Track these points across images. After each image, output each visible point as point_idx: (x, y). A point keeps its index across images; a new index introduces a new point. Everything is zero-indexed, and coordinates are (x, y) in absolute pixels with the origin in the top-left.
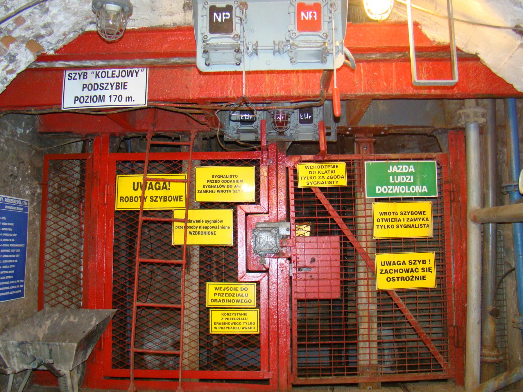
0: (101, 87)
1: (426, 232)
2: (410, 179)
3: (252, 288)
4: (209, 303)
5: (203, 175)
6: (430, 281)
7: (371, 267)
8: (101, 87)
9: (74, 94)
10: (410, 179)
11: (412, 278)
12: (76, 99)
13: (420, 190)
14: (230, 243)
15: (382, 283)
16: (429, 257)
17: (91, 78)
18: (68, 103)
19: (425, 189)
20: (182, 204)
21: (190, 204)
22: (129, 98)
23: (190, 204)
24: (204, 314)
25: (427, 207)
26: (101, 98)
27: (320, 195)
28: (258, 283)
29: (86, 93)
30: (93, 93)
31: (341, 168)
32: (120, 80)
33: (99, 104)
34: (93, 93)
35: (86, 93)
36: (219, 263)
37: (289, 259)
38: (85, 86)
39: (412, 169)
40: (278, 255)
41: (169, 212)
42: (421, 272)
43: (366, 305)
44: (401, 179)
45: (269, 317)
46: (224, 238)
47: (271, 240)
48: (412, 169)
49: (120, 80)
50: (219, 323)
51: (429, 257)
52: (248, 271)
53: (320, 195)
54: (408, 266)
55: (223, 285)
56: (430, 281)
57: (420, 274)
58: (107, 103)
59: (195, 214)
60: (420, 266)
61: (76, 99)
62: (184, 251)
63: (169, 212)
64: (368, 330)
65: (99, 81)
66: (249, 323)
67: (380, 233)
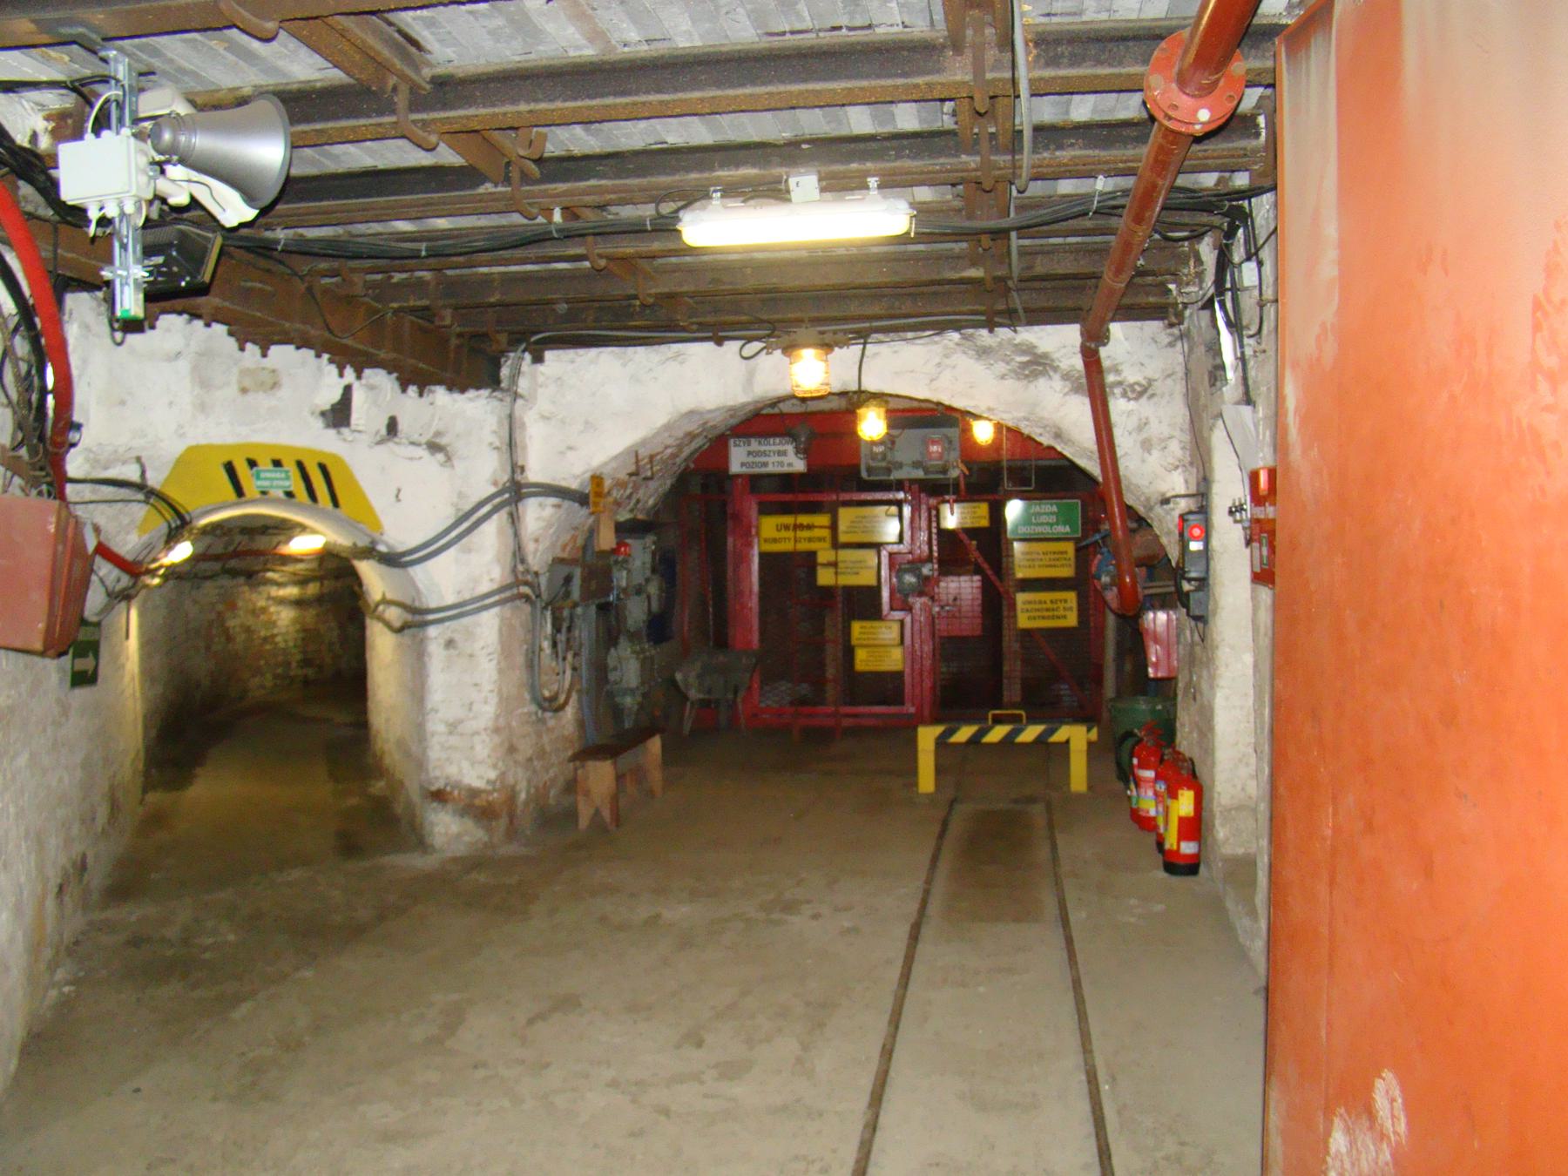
0: (764, 454)
1: (1067, 572)
2: (1053, 519)
3: (896, 627)
4: (854, 642)
5: (846, 516)
6: (1071, 620)
7: (1013, 606)
8: (764, 454)
9: (740, 459)
10: (1053, 519)
11: (1053, 617)
12: (743, 464)
13: (1064, 529)
14: (873, 582)
15: (1023, 622)
16: (1071, 597)
17: (755, 445)
18: (735, 467)
19: (1068, 529)
20: (827, 545)
21: (836, 545)
22: (790, 465)
23: (836, 545)
24: (849, 652)
25: (1070, 548)
26: (765, 464)
27: (964, 537)
28: (902, 623)
29: (751, 459)
30: (758, 459)
31: (983, 509)
32: (781, 448)
33: (763, 470)
34: (758, 459)
35: (751, 459)
36: (864, 603)
37: (932, 598)
38: (749, 453)
39: (1055, 509)
40: (921, 594)
41: (812, 555)
42: (1064, 611)
43: (1010, 644)
44: (1044, 519)
45: (912, 656)
46: (867, 579)
47: (913, 580)
48: (1055, 509)
49: (781, 448)
50: (863, 661)
51: (1071, 597)
52: (892, 609)
53: (964, 537)
54: (1049, 605)
55: (868, 624)
56: (1071, 620)
57: (1061, 613)
58: (770, 469)
59: (845, 555)
60: (1061, 605)
61: (743, 464)
62: (829, 591)
63: (812, 555)
64: (1013, 667)
65: (763, 448)
66: (894, 660)
67: (1020, 575)
